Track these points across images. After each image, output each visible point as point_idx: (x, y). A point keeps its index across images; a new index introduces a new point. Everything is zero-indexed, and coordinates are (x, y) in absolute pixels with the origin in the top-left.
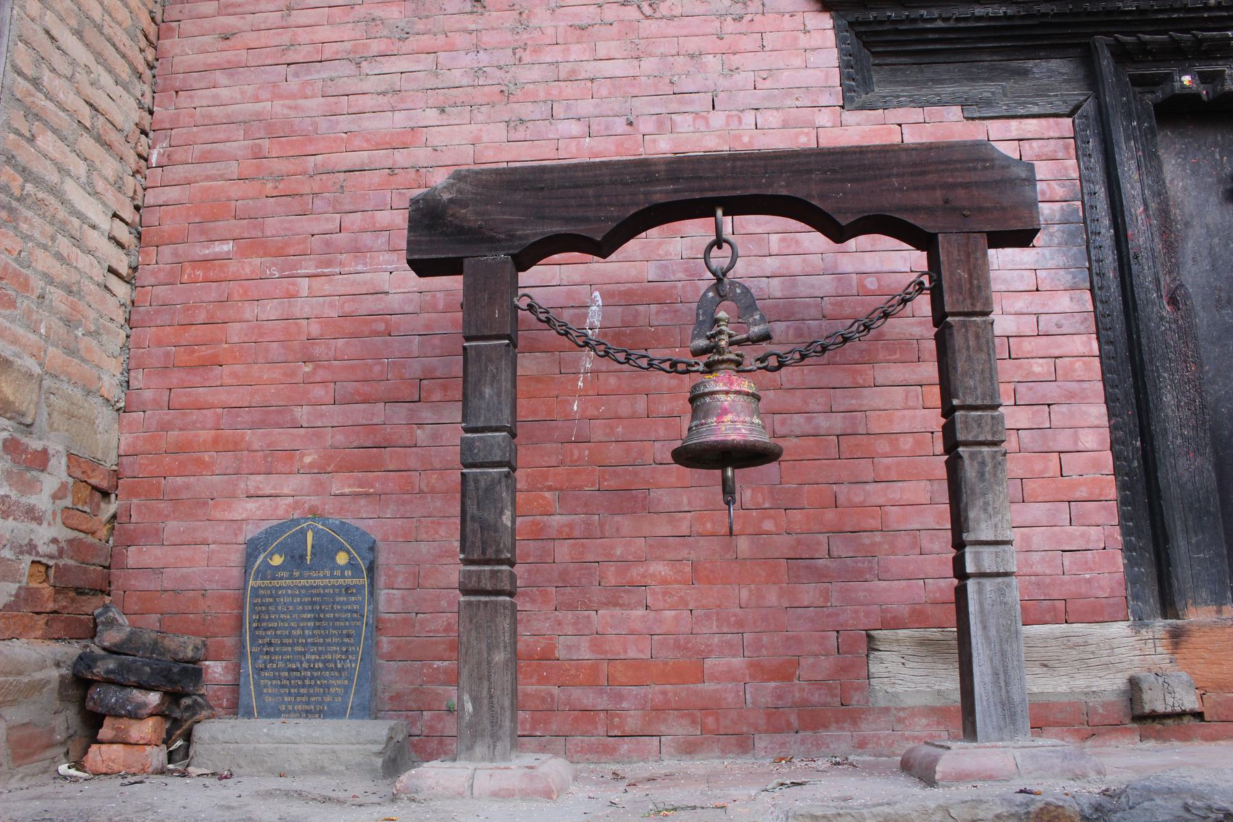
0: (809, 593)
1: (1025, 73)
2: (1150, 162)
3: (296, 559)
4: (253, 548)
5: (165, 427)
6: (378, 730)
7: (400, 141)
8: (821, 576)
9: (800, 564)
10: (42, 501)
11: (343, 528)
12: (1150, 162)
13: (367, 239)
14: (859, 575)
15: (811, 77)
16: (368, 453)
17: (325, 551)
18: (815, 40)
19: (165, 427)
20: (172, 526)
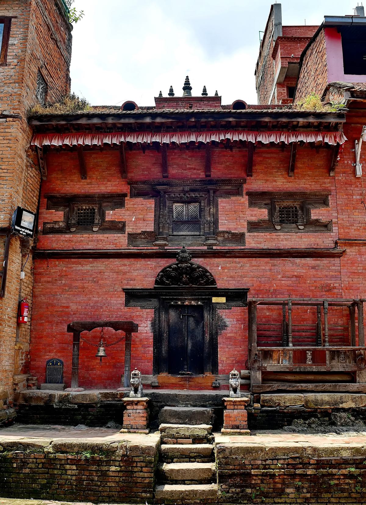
0: (115, 370)
1: (151, 301)
2: (167, 313)
3: (53, 364)
4: (48, 362)
5: (36, 346)
6: (63, 385)
7: (68, 307)
8: (117, 368)
9: (114, 366)
10: (23, 358)
11: (59, 360)
12: (167, 313)
13: (63, 321)
14: (121, 368)
15: (121, 302)
16: (62, 350)
17: (57, 364)
18: (122, 296)
19: (36, 346)
20: (37, 359)
